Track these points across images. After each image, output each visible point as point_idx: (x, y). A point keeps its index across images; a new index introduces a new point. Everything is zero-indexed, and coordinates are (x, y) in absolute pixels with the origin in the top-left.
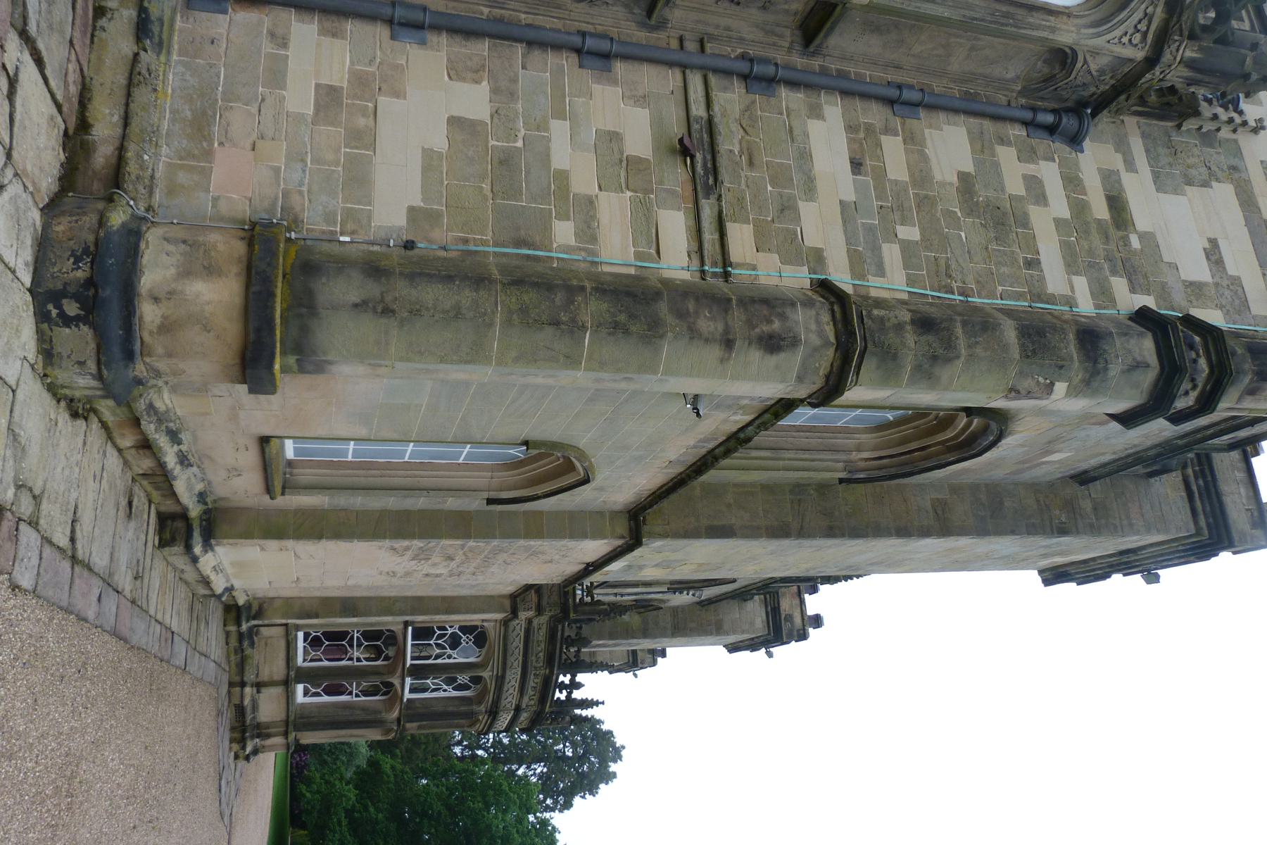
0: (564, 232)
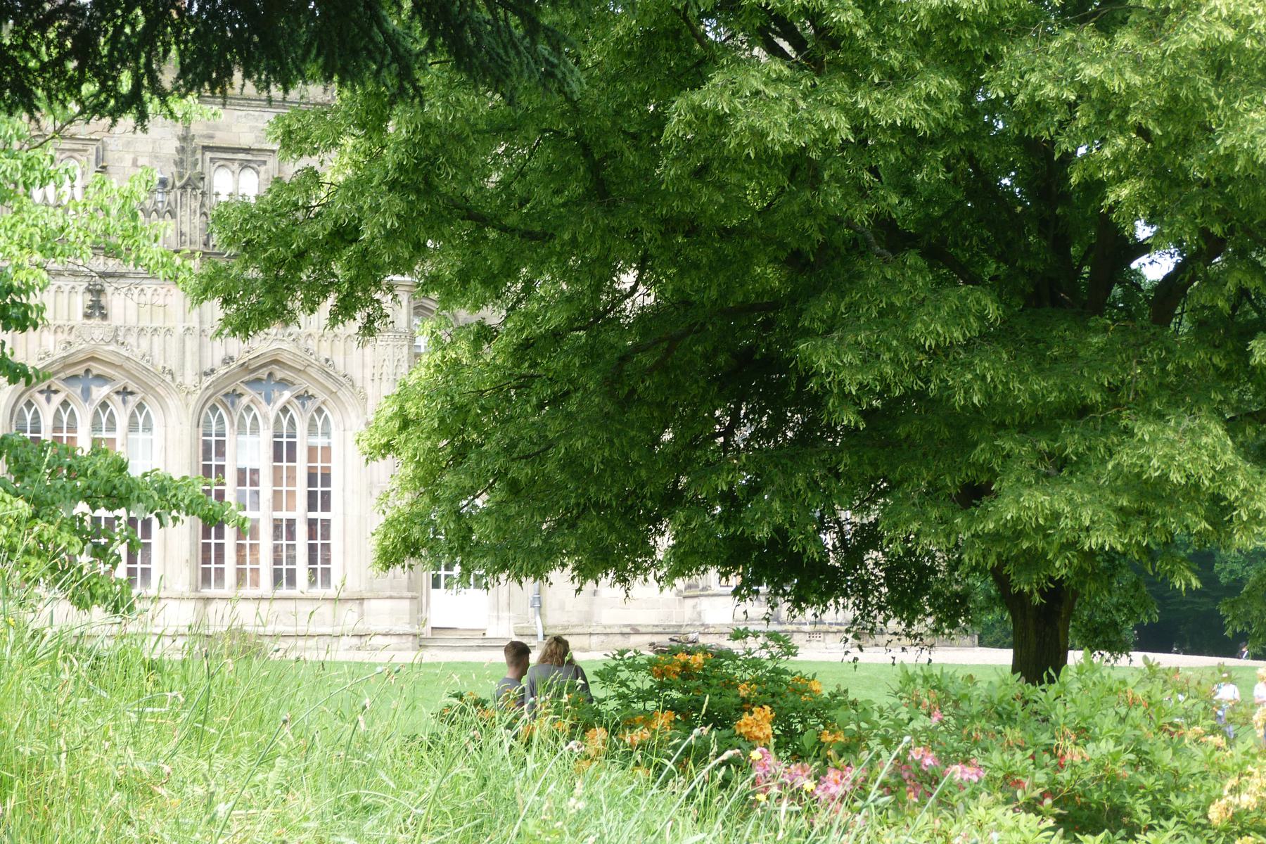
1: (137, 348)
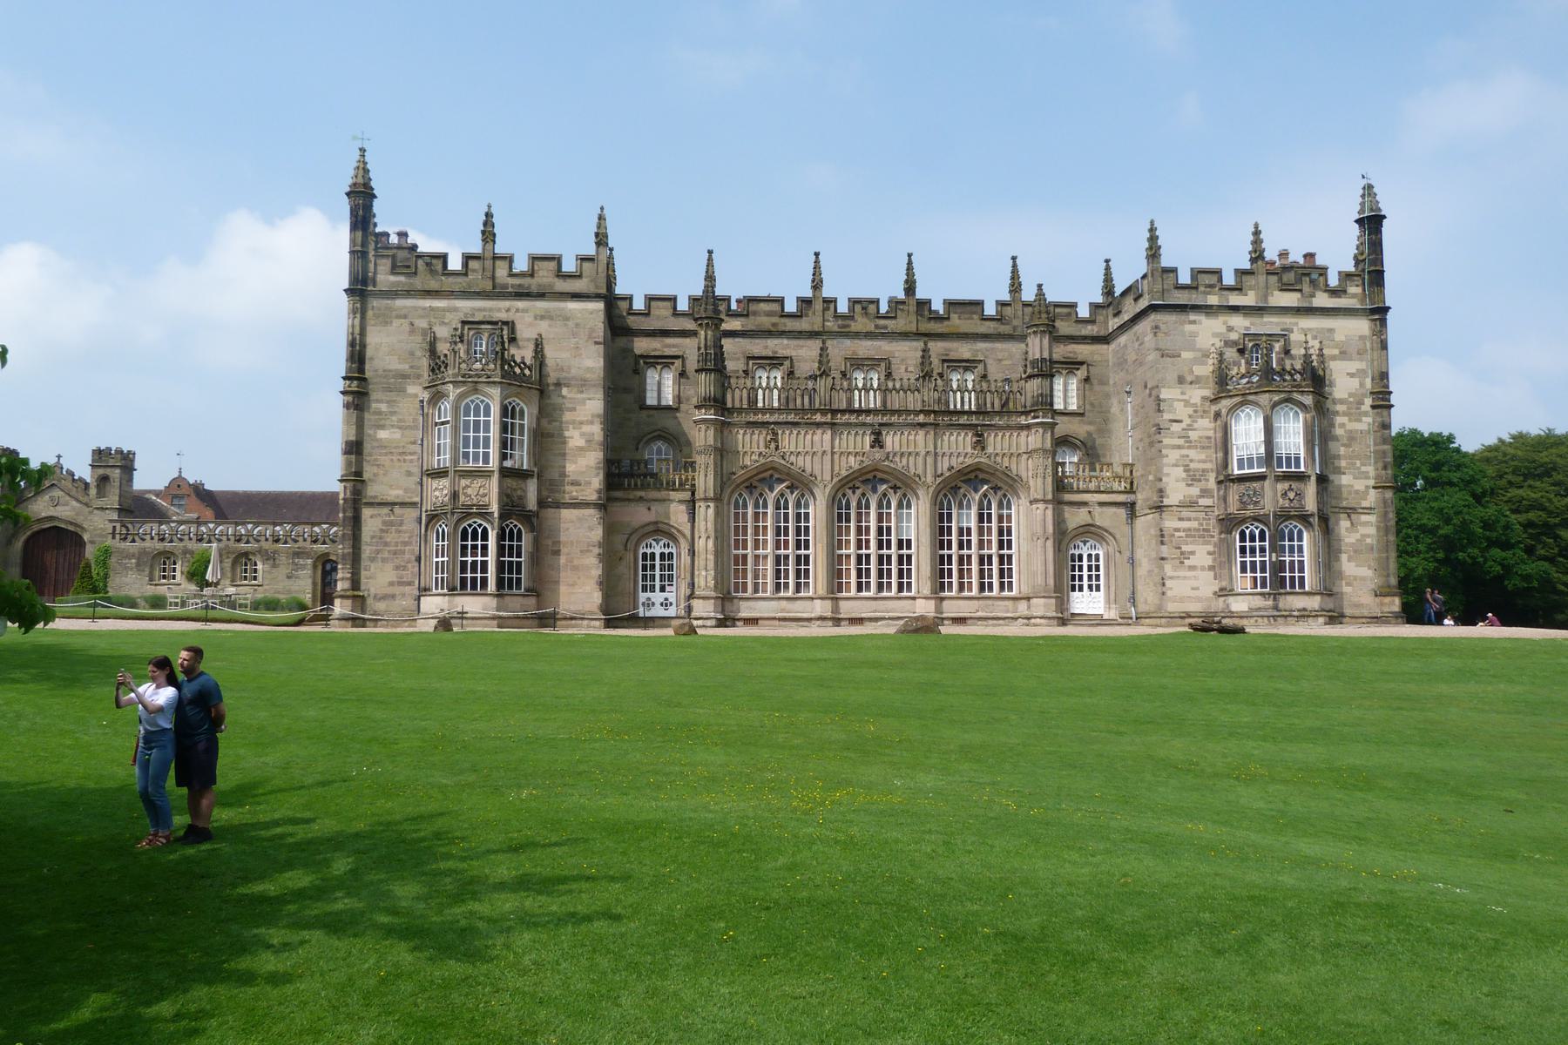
0: (1369, 541)
1: (900, 464)
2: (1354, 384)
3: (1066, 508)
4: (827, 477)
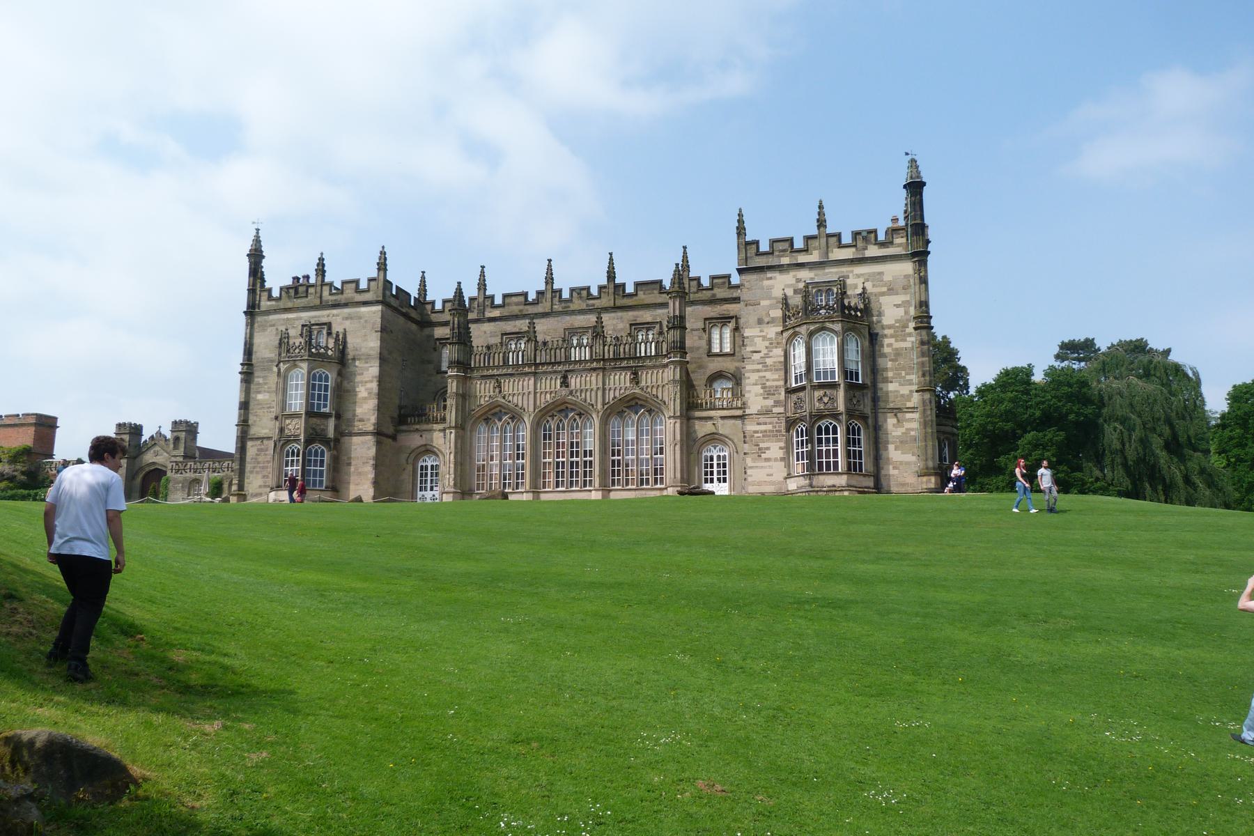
0: (913, 433)
1: (579, 398)
2: (900, 312)
3: (697, 422)
4: (531, 409)
